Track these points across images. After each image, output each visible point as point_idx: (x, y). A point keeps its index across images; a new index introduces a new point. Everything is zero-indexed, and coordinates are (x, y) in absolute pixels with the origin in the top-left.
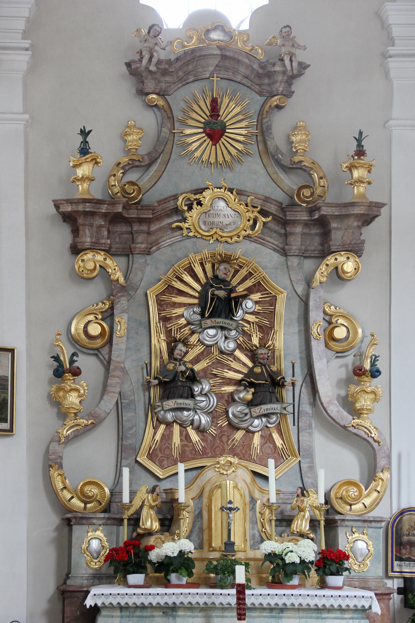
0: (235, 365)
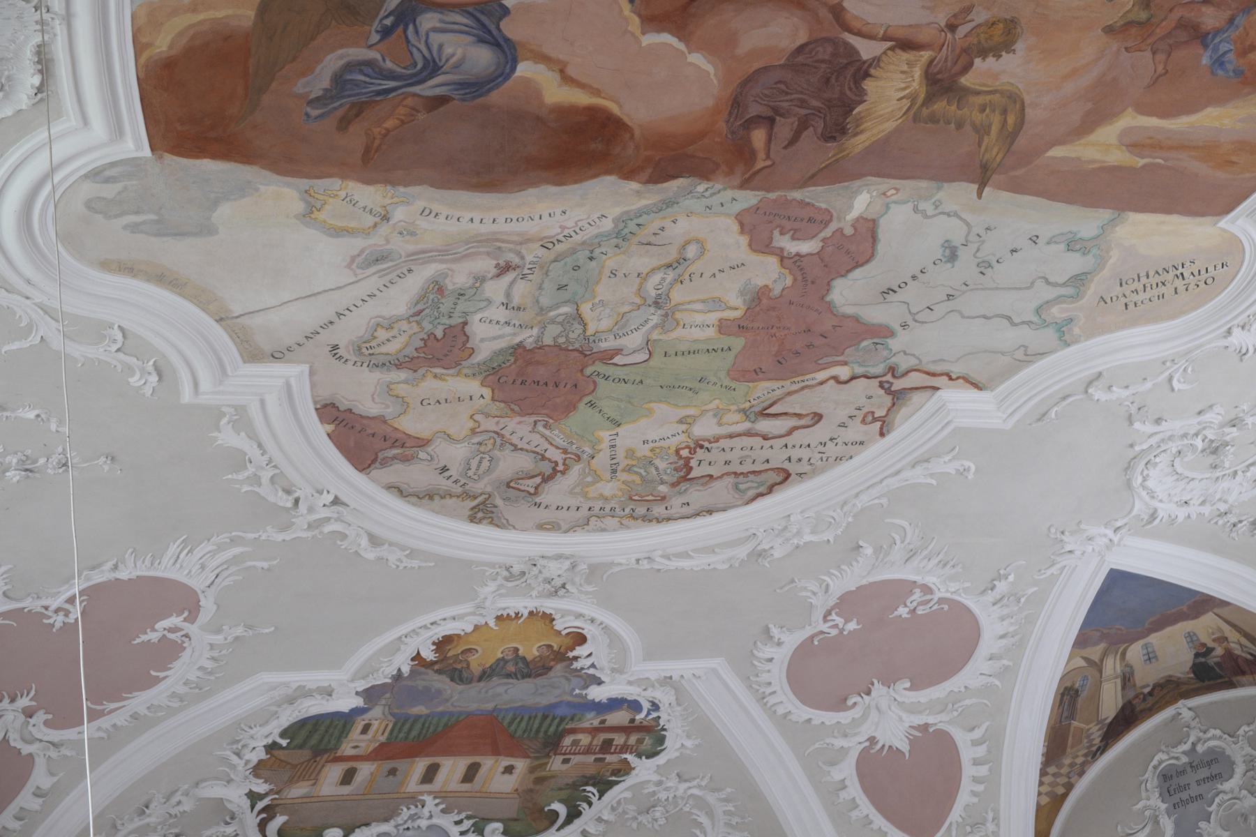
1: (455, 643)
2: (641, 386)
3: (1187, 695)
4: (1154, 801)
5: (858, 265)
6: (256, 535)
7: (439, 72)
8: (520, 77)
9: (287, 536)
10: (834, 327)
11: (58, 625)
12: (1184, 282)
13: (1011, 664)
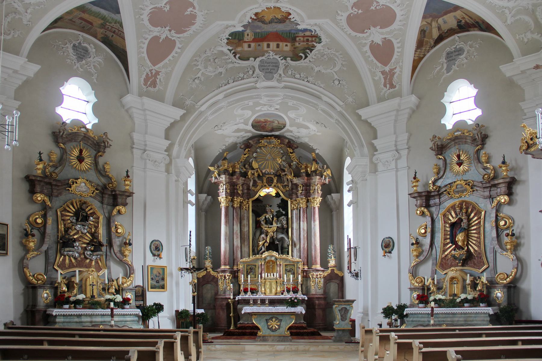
0: (86, 238)
3: (458, 33)
4: (443, 60)
13: (406, 23)
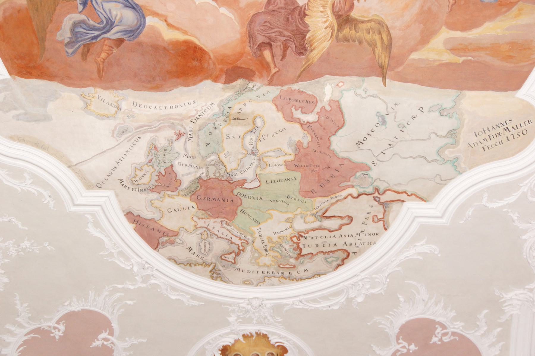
1: (229, 350)
2: (261, 201)
5: (339, 128)
6: (123, 286)
7: (114, 25)
8: (149, 25)
9: (136, 287)
10: (340, 165)
11: (57, 337)
12: (511, 133)
